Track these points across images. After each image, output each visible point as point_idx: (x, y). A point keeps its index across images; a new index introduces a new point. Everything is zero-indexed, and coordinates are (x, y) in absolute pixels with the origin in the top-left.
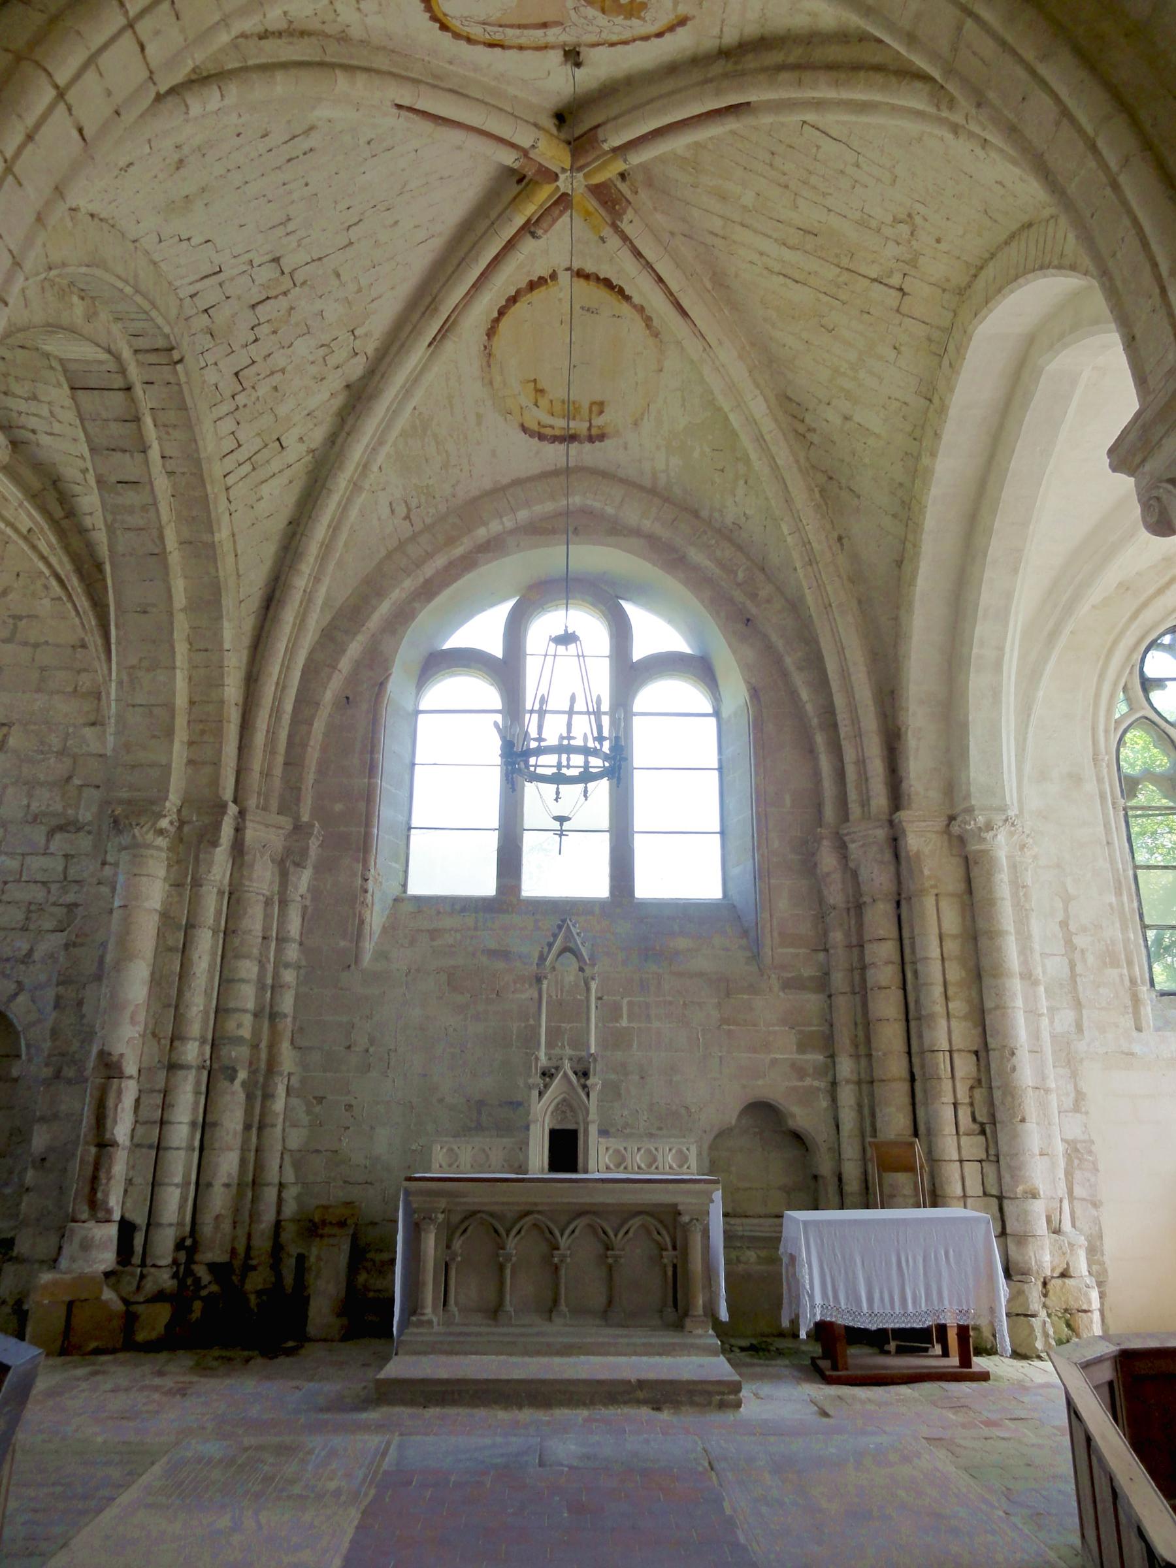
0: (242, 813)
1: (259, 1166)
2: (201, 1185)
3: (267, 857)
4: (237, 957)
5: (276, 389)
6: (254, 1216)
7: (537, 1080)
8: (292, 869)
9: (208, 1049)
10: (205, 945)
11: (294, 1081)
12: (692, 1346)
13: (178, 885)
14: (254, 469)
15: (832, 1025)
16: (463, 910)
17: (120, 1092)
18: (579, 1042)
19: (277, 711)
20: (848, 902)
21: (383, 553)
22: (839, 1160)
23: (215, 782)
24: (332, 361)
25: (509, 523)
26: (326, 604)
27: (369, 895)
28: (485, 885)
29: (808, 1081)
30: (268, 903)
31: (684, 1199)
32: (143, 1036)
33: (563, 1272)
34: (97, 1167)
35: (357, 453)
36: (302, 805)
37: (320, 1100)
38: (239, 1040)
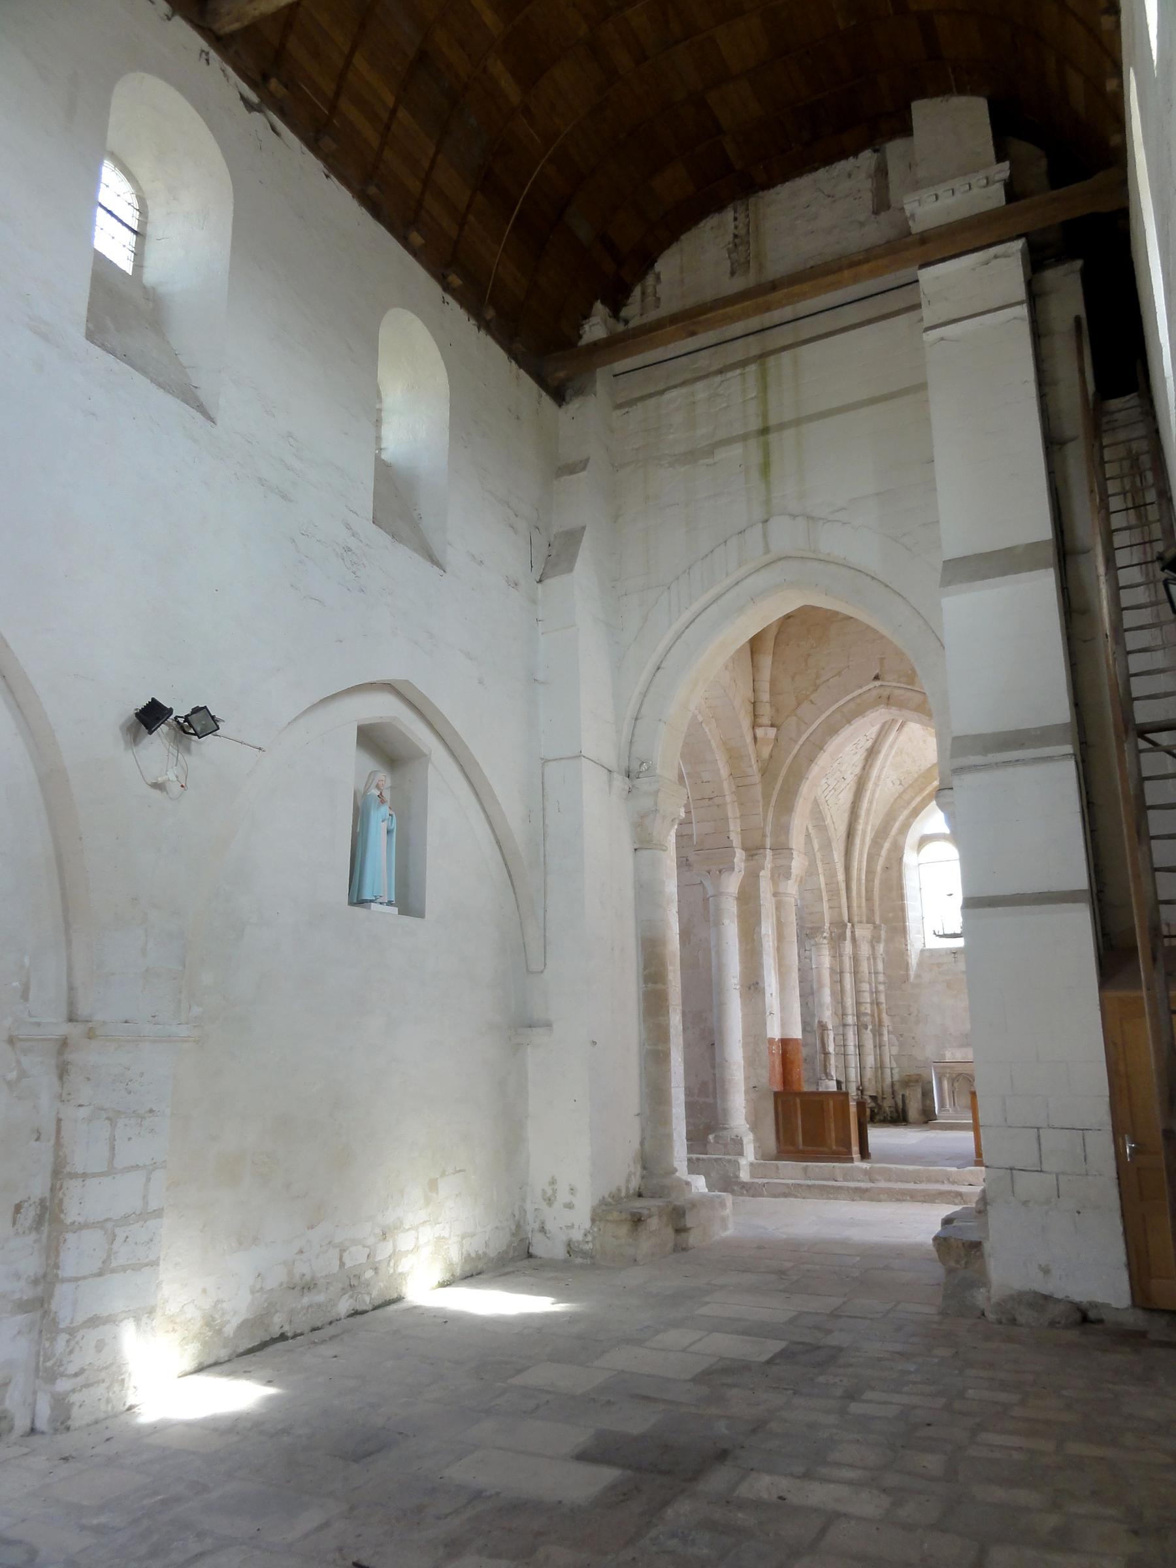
0: (853, 926)
1: (882, 1062)
2: (862, 1068)
3: (865, 942)
4: (860, 982)
5: (839, 763)
6: (883, 1079)
8: (875, 944)
9: (855, 1017)
10: (848, 980)
11: (890, 1028)
13: (834, 957)
14: (835, 791)
17: (828, 1035)
19: (859, 880)
21: (892, 800)
23: (840, 914)
24: (859, 747)
26: (872, 829)
30: (868, 959)
32: (832, 1014)
34: (825, 1061)
35: (875, 773)
36: (875, 916)
37: (901, 1035)
38: (866, 1014)
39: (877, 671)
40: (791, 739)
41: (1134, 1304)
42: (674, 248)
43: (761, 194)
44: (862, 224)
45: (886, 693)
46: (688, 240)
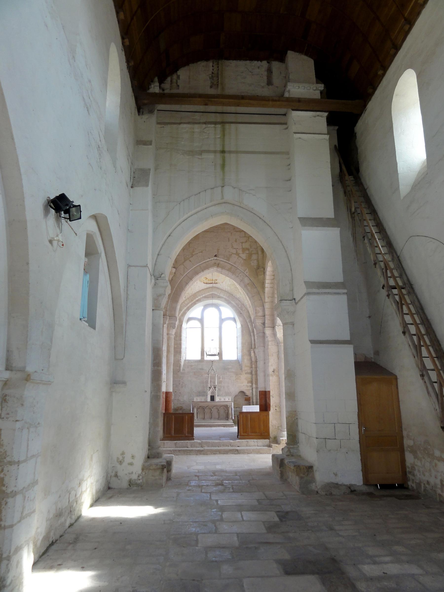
7: (208, 389)
12: (230, 422)
15: (252, 379)
16: (196, 362)
18: (214, 383)
20: (255, 361)
22: (253, 400)
25: (201, 297)
27: (181, 360)
28: (199, 358)
29: (249, 388)
31: (228, 404)
33: (212, 414)
37: (176, 392)
39: (216, 254)
40: (181, 274)
41: (364, 484)
42: (186, 68)
43: (224, 60)
44: (263, 87)
45: (217, 262)
46: (193, 66)
